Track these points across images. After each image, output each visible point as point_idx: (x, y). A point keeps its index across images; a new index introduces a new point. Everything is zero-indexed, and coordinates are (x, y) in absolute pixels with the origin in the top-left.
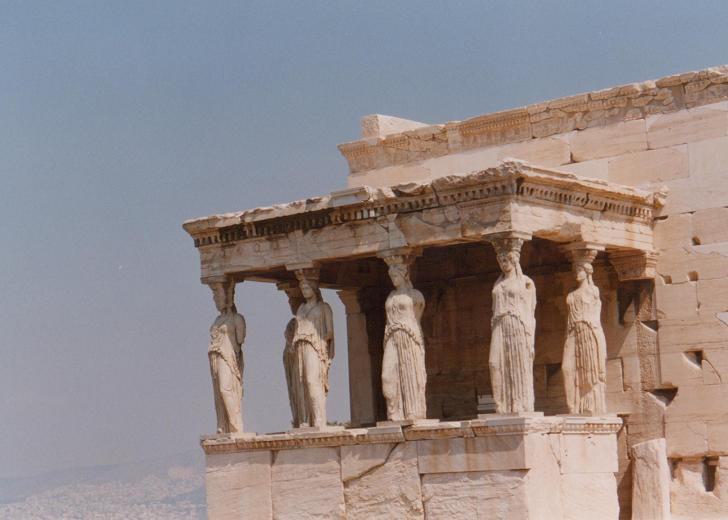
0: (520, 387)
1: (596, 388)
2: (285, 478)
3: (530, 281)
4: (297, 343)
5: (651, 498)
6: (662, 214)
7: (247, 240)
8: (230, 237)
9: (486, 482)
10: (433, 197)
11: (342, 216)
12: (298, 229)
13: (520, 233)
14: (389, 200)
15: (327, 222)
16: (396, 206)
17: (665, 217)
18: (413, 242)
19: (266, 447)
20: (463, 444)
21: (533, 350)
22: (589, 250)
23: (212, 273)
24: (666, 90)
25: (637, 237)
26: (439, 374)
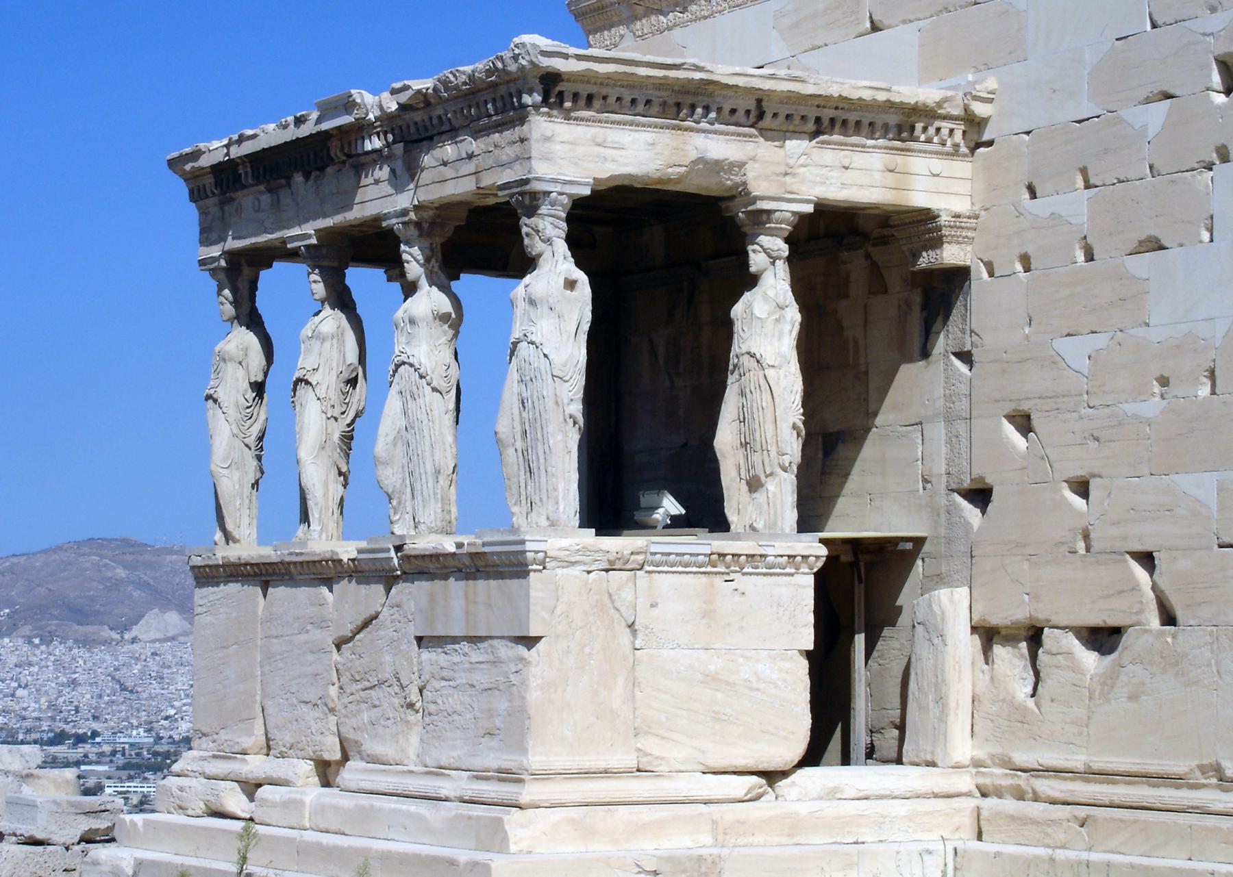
0: (543, 479)
1: (771, 486)
3: (582, 277)
5: (931, 705)
6: (986, 137)
7: (245, 192)
10: (439, 111)
13: (555, 181)
17: (990, 143)
19: (256, 575)
21: (577, 408)
22: (769, 212)
25: (920, 183)
26: (686, 445)
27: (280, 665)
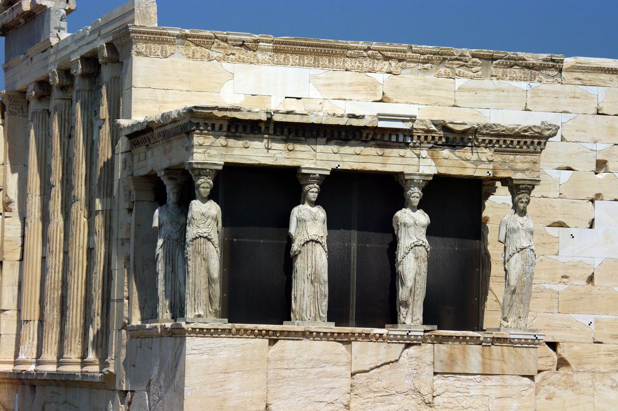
2: (286, 367)
4: (307, 242)
7: (257, 136)
8: (240, 129)
9: (499, 384)
11: (375, 134)
12: (324, 137)
14: (429, 131)
15: (358, 138)
16: (433, 138)
18: (443, 171)
20: (480, 351)
23: (208, 159)
24: (477, 60)
27: (291, 383)
